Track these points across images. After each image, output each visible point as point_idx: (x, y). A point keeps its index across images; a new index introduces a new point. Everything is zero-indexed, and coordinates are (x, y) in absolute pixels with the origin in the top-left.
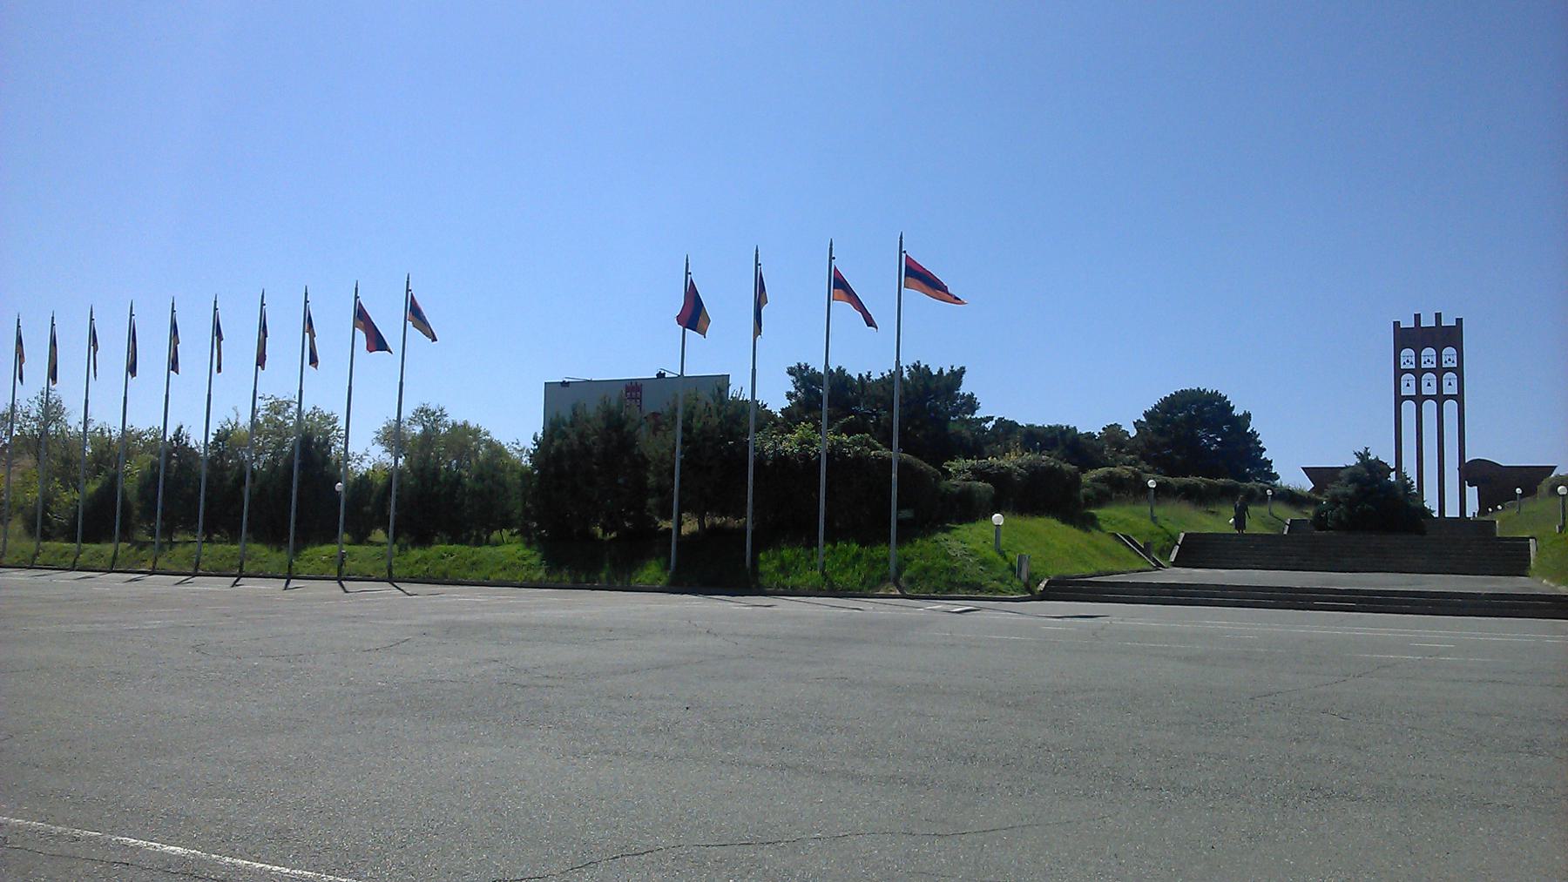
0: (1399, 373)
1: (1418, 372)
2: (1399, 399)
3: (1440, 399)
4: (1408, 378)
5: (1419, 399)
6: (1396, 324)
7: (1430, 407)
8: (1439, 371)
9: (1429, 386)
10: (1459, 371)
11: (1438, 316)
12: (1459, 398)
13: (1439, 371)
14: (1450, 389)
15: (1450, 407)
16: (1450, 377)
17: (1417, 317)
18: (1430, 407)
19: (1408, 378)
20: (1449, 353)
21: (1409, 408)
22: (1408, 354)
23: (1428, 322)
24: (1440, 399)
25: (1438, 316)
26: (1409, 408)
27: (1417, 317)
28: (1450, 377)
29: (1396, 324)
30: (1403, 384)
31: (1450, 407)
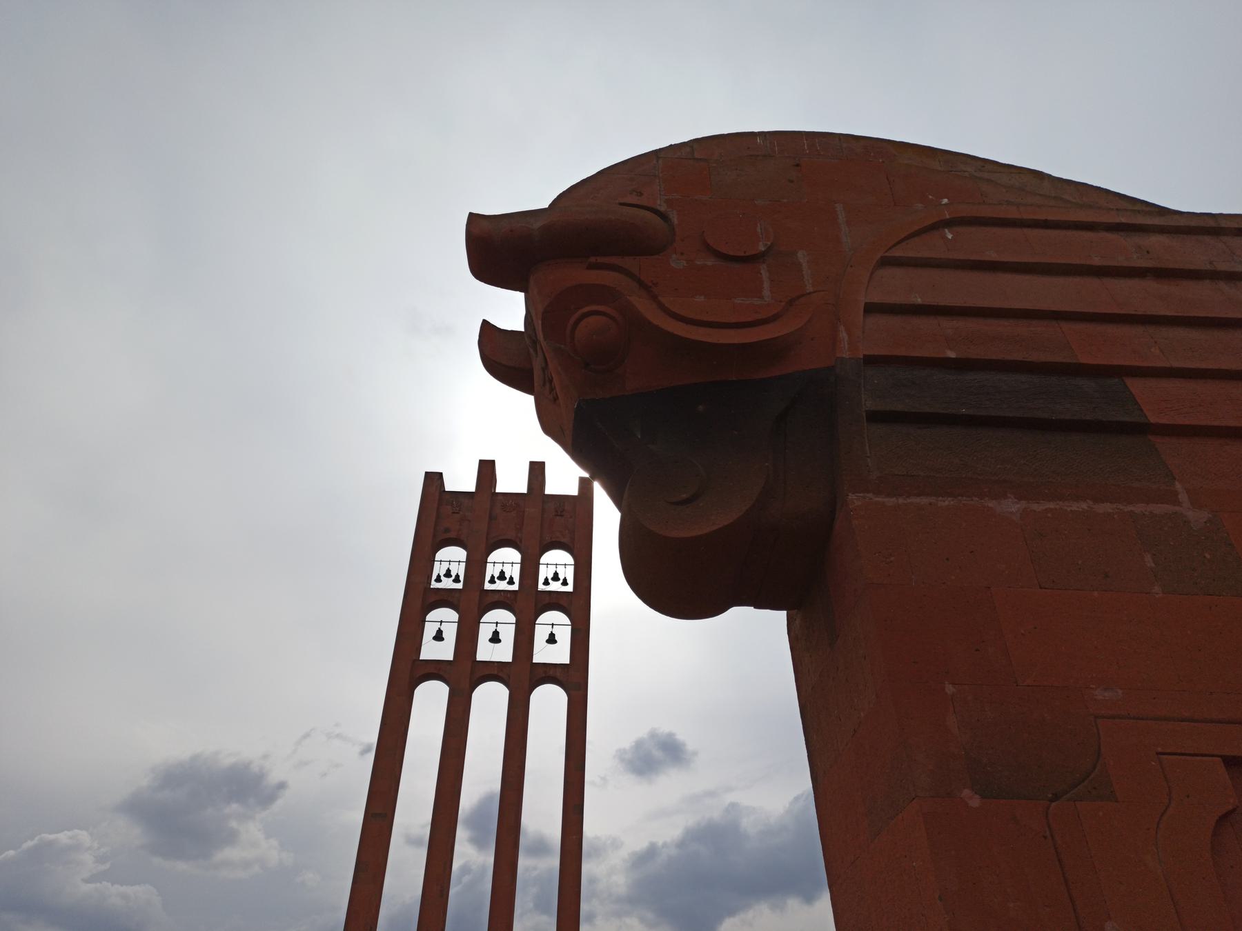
0: (420, 598)
1: (473, 601)
2: (408, 671)
3: (522, 676)
4: (444, 619)
5: (464, 675)
6: (433, 480)
7: (490, 701)
13: (528, 602)
14: (552, 641)
15: (549, 703)
16: (554, 622)
17: (487, 470)
18: (490, 701)
19: (444, 619)
20: (557, 564)
21: (431, 701)
22: (452, 559)
23: (512, 481)
24: (522, 676)
25: (537, 470)
26: (431, 701)
27: (487, 470)
28: (554, 622)
29: (433, 480)
30: (430, 630)
31: (549, 703)
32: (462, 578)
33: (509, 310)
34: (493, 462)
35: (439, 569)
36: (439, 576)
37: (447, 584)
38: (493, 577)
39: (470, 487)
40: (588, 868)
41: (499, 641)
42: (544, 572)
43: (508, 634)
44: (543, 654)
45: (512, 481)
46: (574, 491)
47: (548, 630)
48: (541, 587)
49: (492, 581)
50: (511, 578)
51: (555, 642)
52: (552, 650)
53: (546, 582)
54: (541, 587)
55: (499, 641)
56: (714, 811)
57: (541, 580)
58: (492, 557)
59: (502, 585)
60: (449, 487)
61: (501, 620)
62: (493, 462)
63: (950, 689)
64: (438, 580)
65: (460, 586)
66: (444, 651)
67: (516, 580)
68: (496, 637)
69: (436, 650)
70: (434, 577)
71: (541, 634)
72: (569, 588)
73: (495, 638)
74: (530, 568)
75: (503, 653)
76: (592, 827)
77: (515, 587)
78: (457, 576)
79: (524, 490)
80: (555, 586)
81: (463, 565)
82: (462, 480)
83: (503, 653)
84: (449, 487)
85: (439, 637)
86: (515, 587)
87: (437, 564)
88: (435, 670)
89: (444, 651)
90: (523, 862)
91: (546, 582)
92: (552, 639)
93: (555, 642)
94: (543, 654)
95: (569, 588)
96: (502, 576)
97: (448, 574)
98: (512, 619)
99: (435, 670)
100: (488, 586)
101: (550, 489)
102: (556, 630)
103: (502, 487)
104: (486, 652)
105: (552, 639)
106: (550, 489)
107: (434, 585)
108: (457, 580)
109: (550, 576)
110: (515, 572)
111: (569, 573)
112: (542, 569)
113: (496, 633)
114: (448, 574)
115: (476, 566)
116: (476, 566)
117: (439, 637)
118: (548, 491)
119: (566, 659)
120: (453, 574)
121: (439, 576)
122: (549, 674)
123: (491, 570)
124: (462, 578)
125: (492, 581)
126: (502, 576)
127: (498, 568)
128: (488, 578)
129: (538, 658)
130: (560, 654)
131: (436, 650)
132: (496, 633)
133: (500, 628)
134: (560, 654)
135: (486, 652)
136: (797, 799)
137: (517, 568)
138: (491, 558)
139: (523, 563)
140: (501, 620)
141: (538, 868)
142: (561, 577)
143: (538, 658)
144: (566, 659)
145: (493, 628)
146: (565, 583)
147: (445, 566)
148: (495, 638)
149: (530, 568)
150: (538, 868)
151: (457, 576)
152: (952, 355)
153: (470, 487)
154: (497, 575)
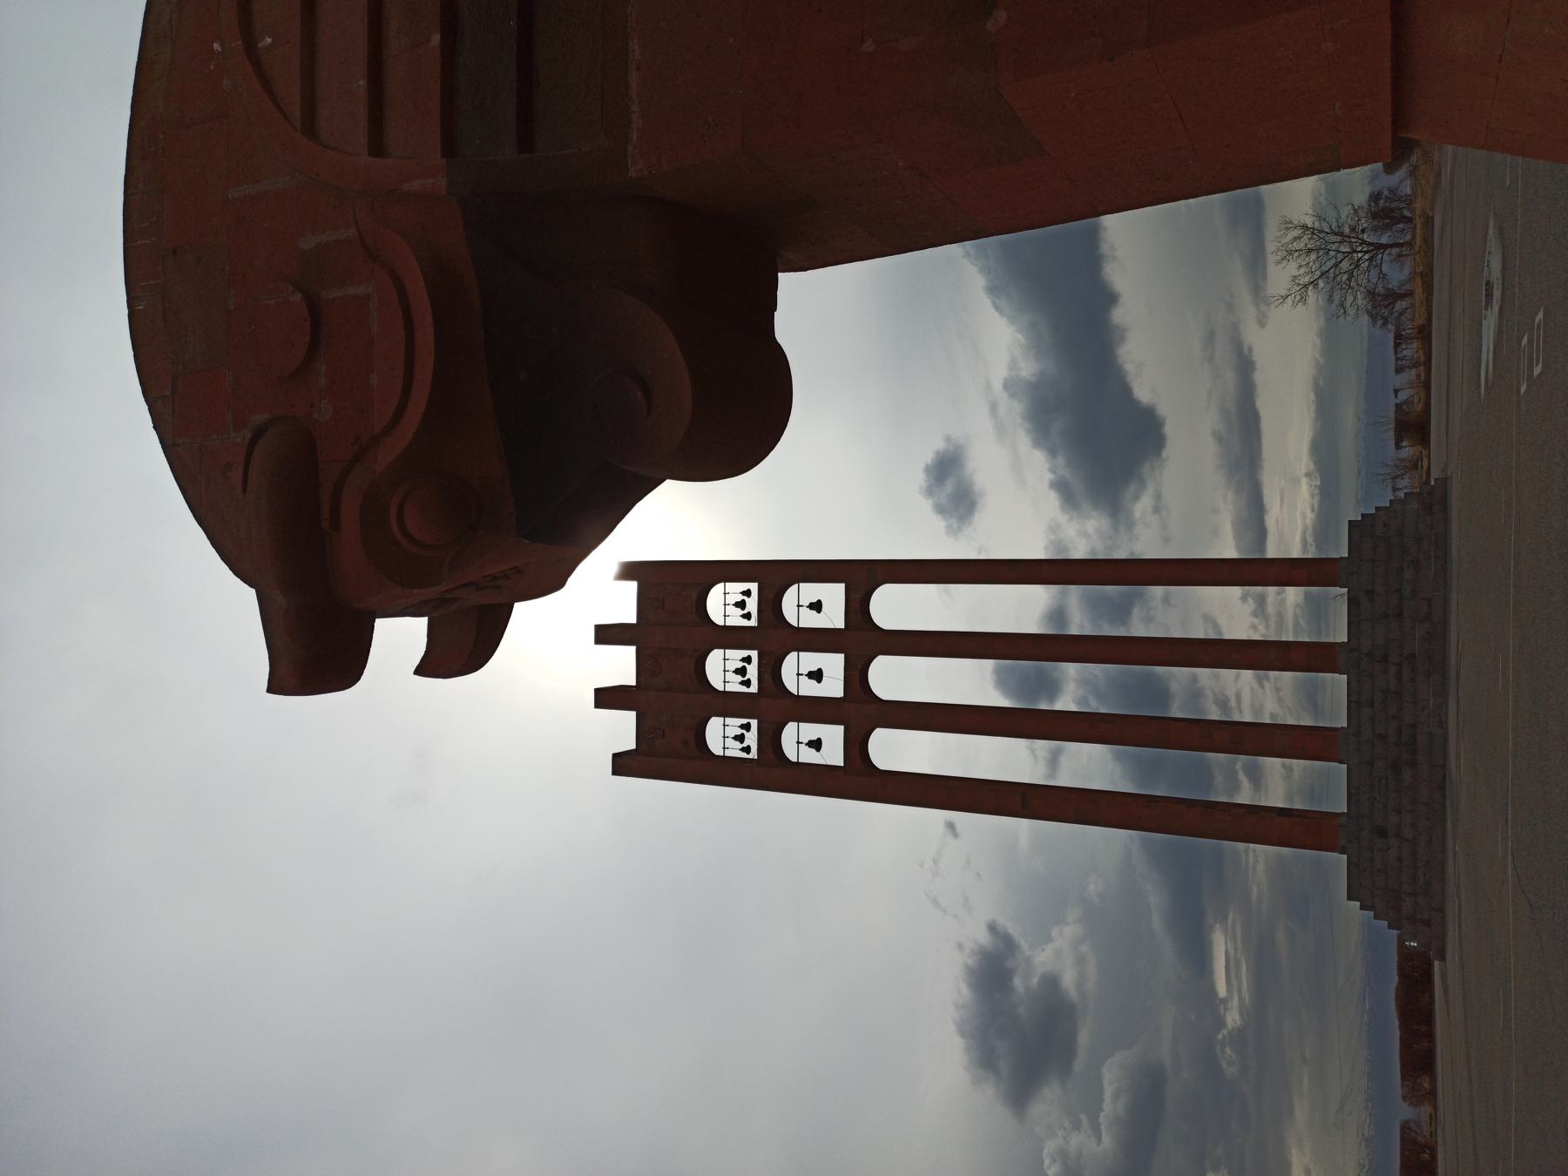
0: (769, 771)
1: (773, 706)
2: (859, 780)
3: (861, 640)
4: (795, 740)
5: (861, 711)
6: (623, 764)
7: (893, 678)
8: (773, 637)
9: (815, 674)
10: (774, 577)
11: (607, 634)
12: (861, 578)
13: (773, 637)
14: (817, 606)
15: (894, 607)
16: (796, 604)
17: (607, 698)
18: (893, 678)
19: (795, 740)
20: (724, 604)
22: (721, 735)
23: (621, 665)
24: (861, 640)
25: (607, 634)
27: (607, 698)
28: (796, 604)
29: (623, 764)
30: (809, 756)
31: (894, 607)
32: (745, 721)
33: (399, 638)
34: (598, 692)
35: (734, 750)
36: (743, 750)
37: (752, 739)
38: (742, 683)
39: (628, 719)
40: (1079, 552)
41: (820, 671)
42: (735, 619)
43: (811, 660)
44: (834, 616)
45: (621, 665)
46: (632, 586)
47: (805, 611)
48: (753, 622)
49: (747, 683)
50: (743, 660)
51: (819, 602)
52: (827, 605)
53: (748, 616)
54: (753, 622)
55: (820, 671)
56: (1012, 410)
57: (745, 623)
58: (718, 684)
59: (753, 671)
60: (631, 744)
61: (795, 670)
62: (598, 692)
63: (869, 46)
64: (747, 750)
65: (754, 723)
66: (833, 737)
67: (745, 653)
68: (815, 674)
69: (832, 745)
70: (744, 755)
71: (810, 620)
72: (754, 587)
73: (817, 675)
74: (730, 637)
75: (833, 664)
76: (1035, 550)
77: (754, 654)
78: (742, 727)
79: (633, 649)
80: (752, 605)
81: (728, 721)
82: (622, 728)
83: (833, 664)
84: (631, 744)
85: (816, 744)
86: (754, 654)
87: (729, 753)
88: (856, 746)
89: (833, 737)
90: (1074, 631)
91: (748, 616)
92: (817, 606)
93: (819, 602)
94: (834, 616)
95: (754, 587)
96: (741, 671)
97: (740, 738)
98: (793, 655)
99: (856, 746)
100: (754, 689)
101: (630, 617)
102: (805, 602)
103: (628, 677)
104: (833, 686)
105: (817, 606)
106: (630, 617)
107: (754, 754)
108: (747, 727)
109: (740, 612)
110: (735, 656)
111: (735, 589)
112: (730, 622)
113: (811, 675)
114: (740, 738)
115: (729, 704)
116: (729, 704)
117: (816, 744)
118: (632, 619)
119: (840, 588)
120: (739, 731)
121: (743, 750)
122: (857, 607)
123: (734, 686)
124: (745, 721)
125: (747, 683)
126: (741, 671)
127: (732, 677)
128: (744, 689)
129: (840, 624)
130: (833, 595)
131: (832, 745)
132: (811, 675)
133: (804, 670)
134: (833, 595)
135: (833, 686)
136: (997, 308)
137: (730, 653)
138: (719, 686)
139: (725, 647)
140: (795, 670)
141: (1079, 611)
142: (740, 598)
143: (840, 624)
144: (840, 588)
145: (804, 679)
146: (748, 593)
147: (731, 743)
148: (817, 675)
149: (730, 637)
150: (1079, 611)
151: (742, 727)
152: (436, 39)
153: (628, 719)
154: (740, 678)
